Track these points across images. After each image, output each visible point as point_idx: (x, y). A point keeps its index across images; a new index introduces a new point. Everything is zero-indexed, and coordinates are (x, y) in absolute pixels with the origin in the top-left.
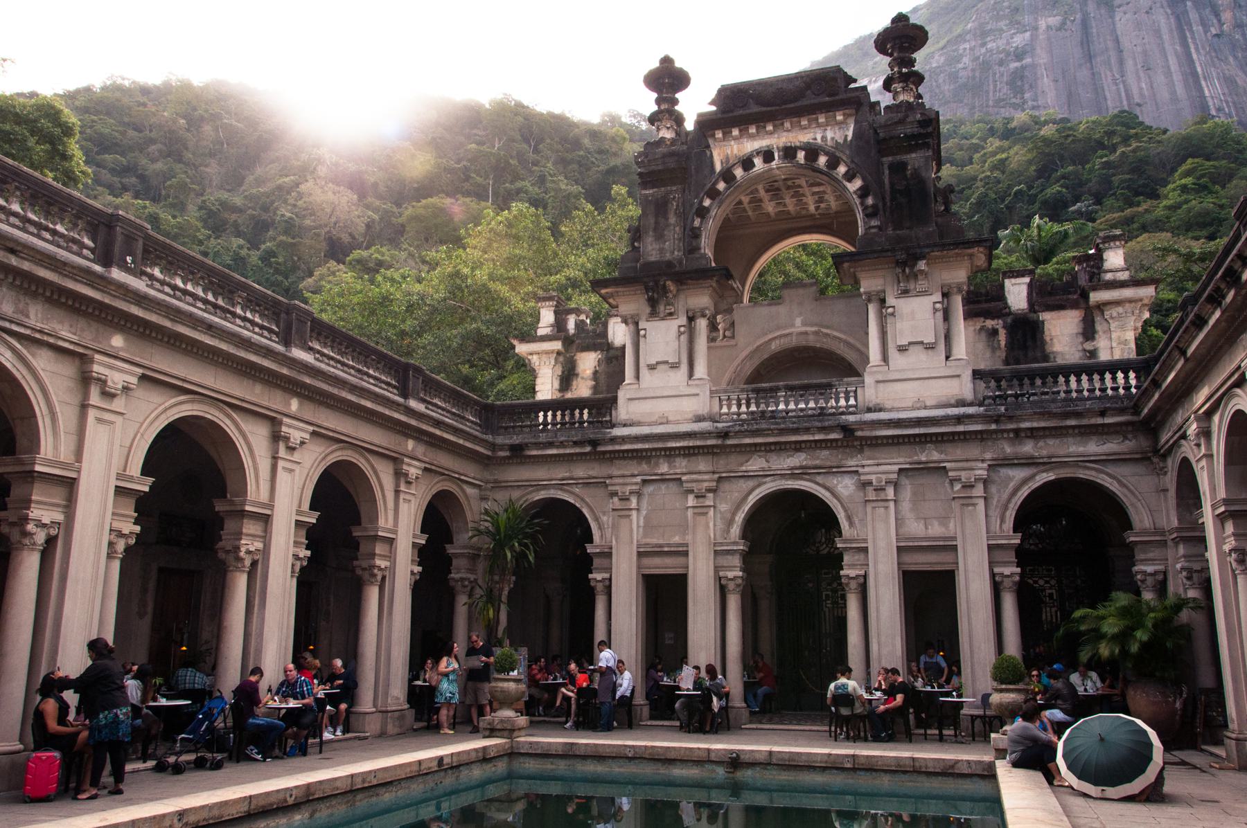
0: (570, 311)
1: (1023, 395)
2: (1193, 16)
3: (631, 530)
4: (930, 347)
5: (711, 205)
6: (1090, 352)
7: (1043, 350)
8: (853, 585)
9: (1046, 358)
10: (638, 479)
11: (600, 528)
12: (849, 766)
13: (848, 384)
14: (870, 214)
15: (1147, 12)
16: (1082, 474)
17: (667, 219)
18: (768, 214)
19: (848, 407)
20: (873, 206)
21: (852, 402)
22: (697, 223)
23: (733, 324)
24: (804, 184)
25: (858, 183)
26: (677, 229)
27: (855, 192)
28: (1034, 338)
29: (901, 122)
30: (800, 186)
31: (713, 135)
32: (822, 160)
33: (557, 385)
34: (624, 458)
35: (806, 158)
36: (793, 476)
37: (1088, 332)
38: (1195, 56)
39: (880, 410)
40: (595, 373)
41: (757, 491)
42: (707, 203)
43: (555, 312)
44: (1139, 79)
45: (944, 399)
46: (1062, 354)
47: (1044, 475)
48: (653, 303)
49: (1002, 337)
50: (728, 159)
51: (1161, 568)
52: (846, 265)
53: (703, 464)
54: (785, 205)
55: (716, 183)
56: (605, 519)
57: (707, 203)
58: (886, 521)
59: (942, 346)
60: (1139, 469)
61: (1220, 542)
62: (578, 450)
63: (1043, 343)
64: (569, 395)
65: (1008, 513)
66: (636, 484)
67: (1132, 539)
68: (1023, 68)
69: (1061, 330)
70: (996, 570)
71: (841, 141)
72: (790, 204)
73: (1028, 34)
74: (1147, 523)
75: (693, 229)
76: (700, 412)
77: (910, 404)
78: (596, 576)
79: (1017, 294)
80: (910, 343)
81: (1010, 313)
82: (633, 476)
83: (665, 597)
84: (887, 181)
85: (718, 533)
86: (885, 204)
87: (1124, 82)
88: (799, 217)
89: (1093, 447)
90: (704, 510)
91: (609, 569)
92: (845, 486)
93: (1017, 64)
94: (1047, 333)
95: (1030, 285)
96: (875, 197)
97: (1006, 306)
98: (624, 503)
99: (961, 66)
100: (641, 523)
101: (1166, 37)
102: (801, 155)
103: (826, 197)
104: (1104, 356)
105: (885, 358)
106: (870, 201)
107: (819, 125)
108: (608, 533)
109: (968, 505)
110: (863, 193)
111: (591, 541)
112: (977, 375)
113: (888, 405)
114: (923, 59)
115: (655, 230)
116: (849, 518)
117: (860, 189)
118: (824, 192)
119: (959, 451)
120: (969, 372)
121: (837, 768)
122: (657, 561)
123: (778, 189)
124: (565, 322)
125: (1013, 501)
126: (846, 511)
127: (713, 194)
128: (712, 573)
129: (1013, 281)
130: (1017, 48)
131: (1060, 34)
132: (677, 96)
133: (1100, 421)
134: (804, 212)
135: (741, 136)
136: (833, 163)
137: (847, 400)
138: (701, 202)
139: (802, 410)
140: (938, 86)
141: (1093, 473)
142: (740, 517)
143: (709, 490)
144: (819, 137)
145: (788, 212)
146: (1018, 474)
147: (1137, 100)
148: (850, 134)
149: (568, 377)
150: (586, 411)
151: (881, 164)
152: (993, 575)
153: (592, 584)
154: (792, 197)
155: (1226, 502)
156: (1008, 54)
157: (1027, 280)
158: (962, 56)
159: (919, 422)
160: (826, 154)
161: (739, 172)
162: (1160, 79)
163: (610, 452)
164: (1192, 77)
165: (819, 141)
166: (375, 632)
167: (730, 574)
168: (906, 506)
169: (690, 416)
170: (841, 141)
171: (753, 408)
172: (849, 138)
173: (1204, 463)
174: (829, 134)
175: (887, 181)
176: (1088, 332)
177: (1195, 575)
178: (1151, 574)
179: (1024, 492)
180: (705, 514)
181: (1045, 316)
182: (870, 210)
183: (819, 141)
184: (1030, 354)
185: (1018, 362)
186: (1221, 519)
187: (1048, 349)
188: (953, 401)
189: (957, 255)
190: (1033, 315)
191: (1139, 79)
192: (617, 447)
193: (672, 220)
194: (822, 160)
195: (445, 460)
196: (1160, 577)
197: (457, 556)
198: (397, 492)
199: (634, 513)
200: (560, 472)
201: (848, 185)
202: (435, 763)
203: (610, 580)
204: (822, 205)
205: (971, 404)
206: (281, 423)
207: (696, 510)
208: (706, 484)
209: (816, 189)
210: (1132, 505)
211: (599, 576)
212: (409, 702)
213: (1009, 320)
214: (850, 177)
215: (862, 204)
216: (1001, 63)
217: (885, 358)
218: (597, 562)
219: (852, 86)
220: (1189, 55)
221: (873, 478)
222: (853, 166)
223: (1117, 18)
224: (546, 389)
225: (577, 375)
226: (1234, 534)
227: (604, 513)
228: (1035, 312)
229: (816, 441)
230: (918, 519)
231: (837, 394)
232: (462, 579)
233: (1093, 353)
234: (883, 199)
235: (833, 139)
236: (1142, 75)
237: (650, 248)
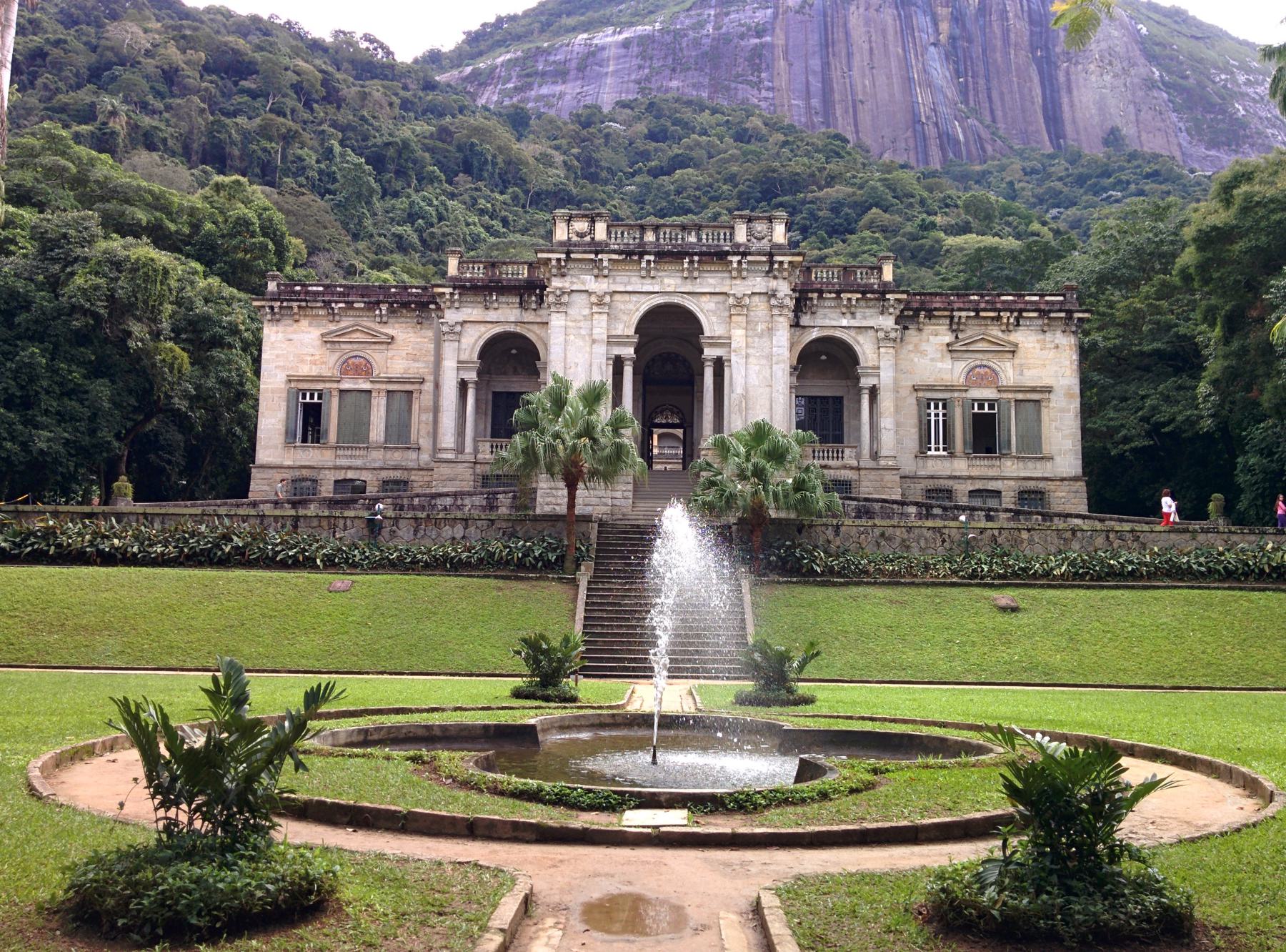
15: (877, 10)
44: (864, 76)
68: (763, 45)
73: (769, 11)
87: (850, 77)
93: (757, 41)
99: (705, 32)
101: (891, 37)
130: (758, 24)
131: (799, 17)
140: (681, 50)
147: (860, 97)
156: (749, 29)
158: (706, 22)
162: (881, 80)
191: (864, 76)
216: (742, 37)
236: (867, 72)
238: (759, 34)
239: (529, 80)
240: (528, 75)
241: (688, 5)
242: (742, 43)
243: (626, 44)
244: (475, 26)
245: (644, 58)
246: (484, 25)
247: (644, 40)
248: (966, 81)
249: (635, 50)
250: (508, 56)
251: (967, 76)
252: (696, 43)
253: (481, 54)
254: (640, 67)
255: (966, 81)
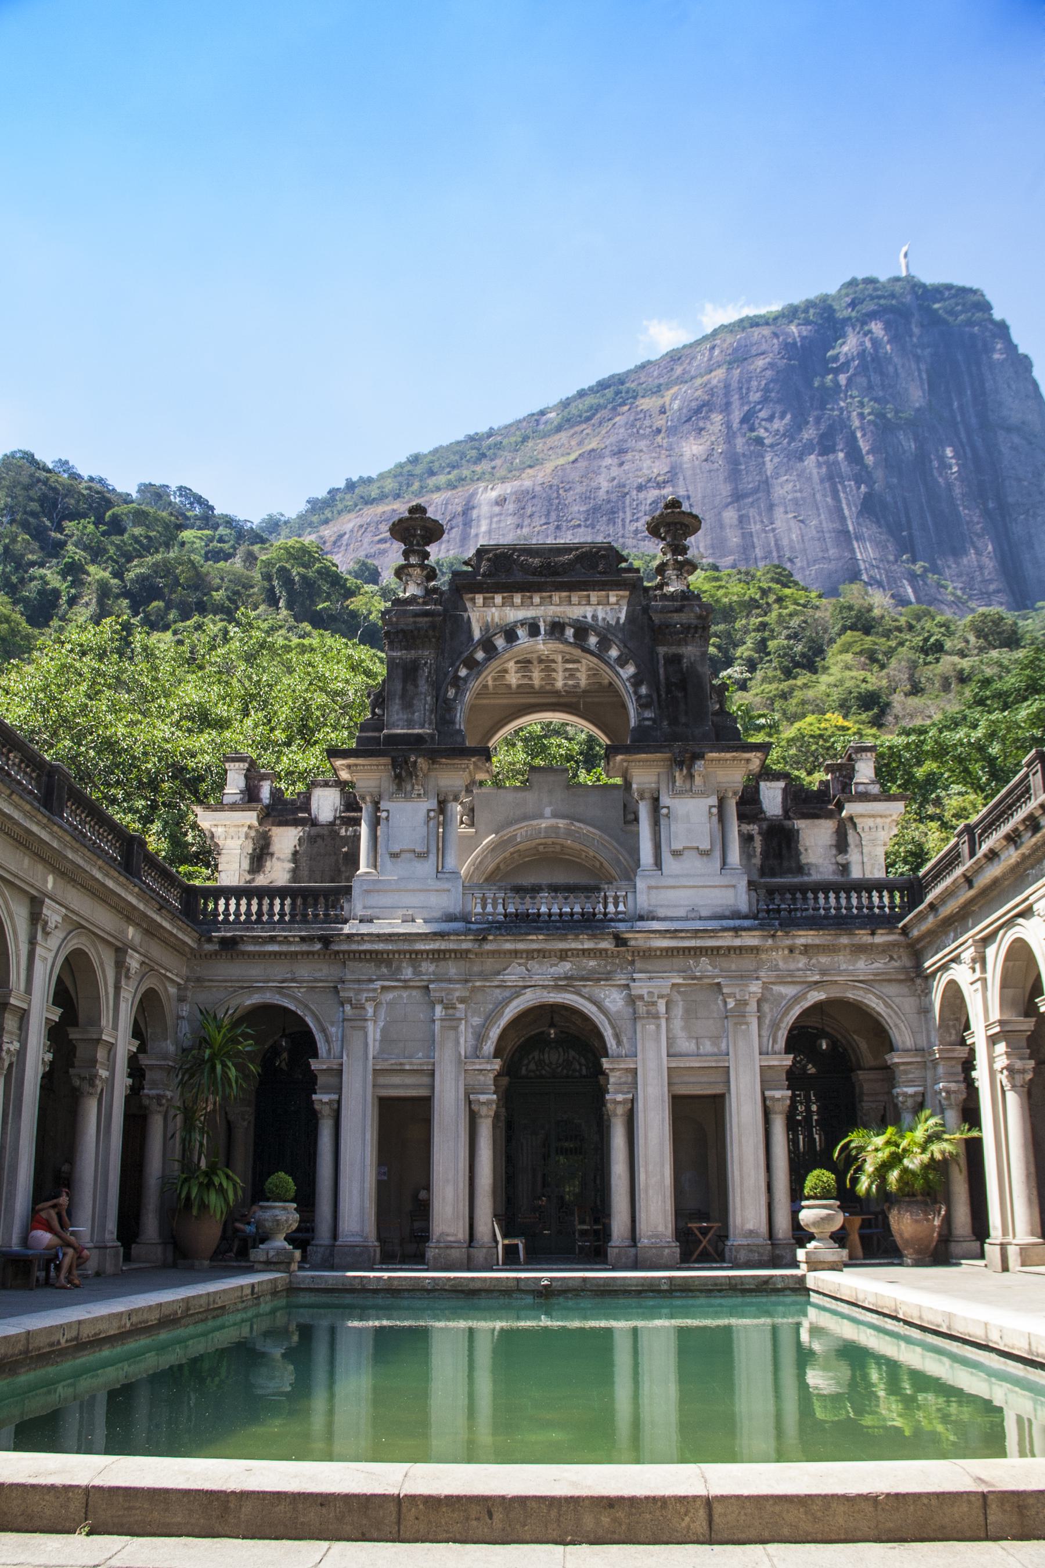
0: (264, 777)
1: (796, 910)
2: (845, 468)
3: (366, 1045)
4: (705, 854)
5: (467, 676)
6: (843, 866)
7: (798, 861)
8: (620, 1110)
9: (800, 869)
10: (378, 984)
11: (327, 1041)
12: (665, 1287)
13: (618, 889)
14: (643, 704)
16: (850, 995)
17: (416, 686)
18: (509, 686)
19: (617, 913)
20: (648, 696)
21: (621, 908)
22: (451, 693)
23: (472, 810)
24: (559, 659)
25: (631, 670)
26: (429, 699)
27: (628, 680)
28: (789, 847)
29: (679, 610)
30: (554, 661)
31: (473, 600)
32: (593, 640)
33: (246, 865)
34: (360, 960)
35: (575, 636)
36: (557, 988)
37: (841, 845)
38: (846, 512)
39: (653, 919)
40: (295, 853)
41: (514, 1003)
42: (463, 672)
43: (246, 776)
45: (719, 910)
46: (816, 866)
47: (815, 993)
48: (399, 780)
49: (758, 843)
50: (487, 630)
51: (920, 1089)
52: (619, 758)
53: (452, 969)
54: (530, 678)
55: (474, 651)
56: (333, 1030)
57: (463, 672)
58: (658, 1040)
59: (717, 854)
60: (904, 989)
61: (991, 1060)
62: (305, 948)
63: (798, 854)
64: (261, 880)
65: (780, 1034)
66: (375, 990)
67: (896, 1060)
69: (815, 838)
70: (768, 1093)
71: (613, 622)
72: (537, 677)
74: (909, 1043)
75: (446, 701)
76: (451, 910)
77: (681, 913)
78: (322, 1097)
79: (772, 797)
80: (685, 848)
81: (765, 819)
82: (371, 981)
83: (404, 1125)
84: (661, 671)
85: (469, 1049)
86: (659, 696)
88: (542, 692)
89: (862, 966)
90: (454, 1023)
91: (339, 1090)
92: (614, 1000)
93: (656, 492)
94: (801, 842)
95: (785, 791)
96: (649, 687)
97: (762, 811)
98: (357, 1011)
100: (378, 1037)
102: (570, 632)
103: (578, 674)
104: (856, 873)
105: (658, 863)
106: (643, 690)
107: (589, 604)
108: (336, 1047)
109: (741, 1024)
110: (637, 681)
111: (315, 1055)
112: (750, 883)
113: (661, 912)
114: (697, 545)
115: (403, 696)
116: (617, 1036)
117: (634, 676)
118: (577, 670)
119: (734, 964)
120: (743, 883)
121: (652, 1291)
122: (396, 1080)
123: (529, 662)
124: (258, 788)
125: (786, 1020)
126: (613, 1028)
127: (472, 664)
128: (462, 1096)
129: (768, 784)
131: (707, 466)
132: (428, 549)
133: (868, 939)
134: (548, 687)
135: (503, 605)
136: (604, 643)
137: (616, 906)
138: (457, 671)
139: (566, 913)
141: (861, 993)
142: (495, 1033)
143: (462, 1000)
144: (589, 616)
145: (532, 686)
146: (789, 991)
148: (623, 616)
149: (260, 856)
150: (288, 901)
151: (653, 653)
152: (764, 1099)
153: (317, 1107)
154: (542, 670)
155: (1001, 1023)
157: (782, 784)
159: (696, 933)
160: (597, 634)
161: (500, 642)
163: (344, 952)
164: (844, 537)
165: (589, 619)
166: (93, 1155)
167: (483, 1098)
168: (678, 1024)
169: (437, 914)
170: (613, 622)
171: (511, 909)
172: (622, 621)
173: (978, 985)
174: (601, 615)
175: (661, 671)
176: (841, 845)
177: (953, 1096)
178: (911, 1096)
179: (797, 1011)
180: (456, 1028)
181: (800, 824)
182: (643, 701)
183: (589, 619)
184: (785, 864)
185: (773, 875)
186: (993, 1040)
187: (804, 860)
188: (727, 913)
189: (734, 759)
190: (787, 823)
192: (354, 947)
193: (423, 687)
194: (593, 640)
195: (157, 951)
196: (919, 1099)
197: (152, 1067)
198: (117, 988)
199: (370, 1025)
200: (280, 971)
201: (621, 671)
202: (249, 1291)
203: (339, 1102)
204: (570, 682)
205: (746, 917)
206: (42, 902)
207: (447, 1024)
208: (457, 994)
209: (570, 666)
210: (896, 1025)
211: (325, 1098)
212: (119, 1239)
213: (765, 825)
214: (622, 662)
215: (636, 692)
216: (640, 488)
217: (658, 863)
218: (321, 1080)
219: (624, 565)
220: (840, 510)
221: (644, 992)
222: (626, 651)
223: (768, 459)
224: (231, 871)
225: (272, 855)
226: (1007, 1053)
227: (332, 1024)
228: (789, 819)
229: (584, 950)
230: (690, 1038)
231: (606, 897)
232: (159, 1097)
233: (845, 868)
234: (658, 690)
235: (604, 619)
237: (396, 717)
238: (659, 486)
239: (383, 546)
240: (380, 541)
241: (572, 457)
242: (642, 495)
243: (501, 502)
244: (322, 494)
245: (522, 516)
246: (333, 492)
247: (524, 498)
248: (911, 535)
249: (511, 507)
250: (359, 521)
251: (910, 528)
252: (585, 498)
253: (326, 522)
254: (519, 526)
255: (911, 535)
